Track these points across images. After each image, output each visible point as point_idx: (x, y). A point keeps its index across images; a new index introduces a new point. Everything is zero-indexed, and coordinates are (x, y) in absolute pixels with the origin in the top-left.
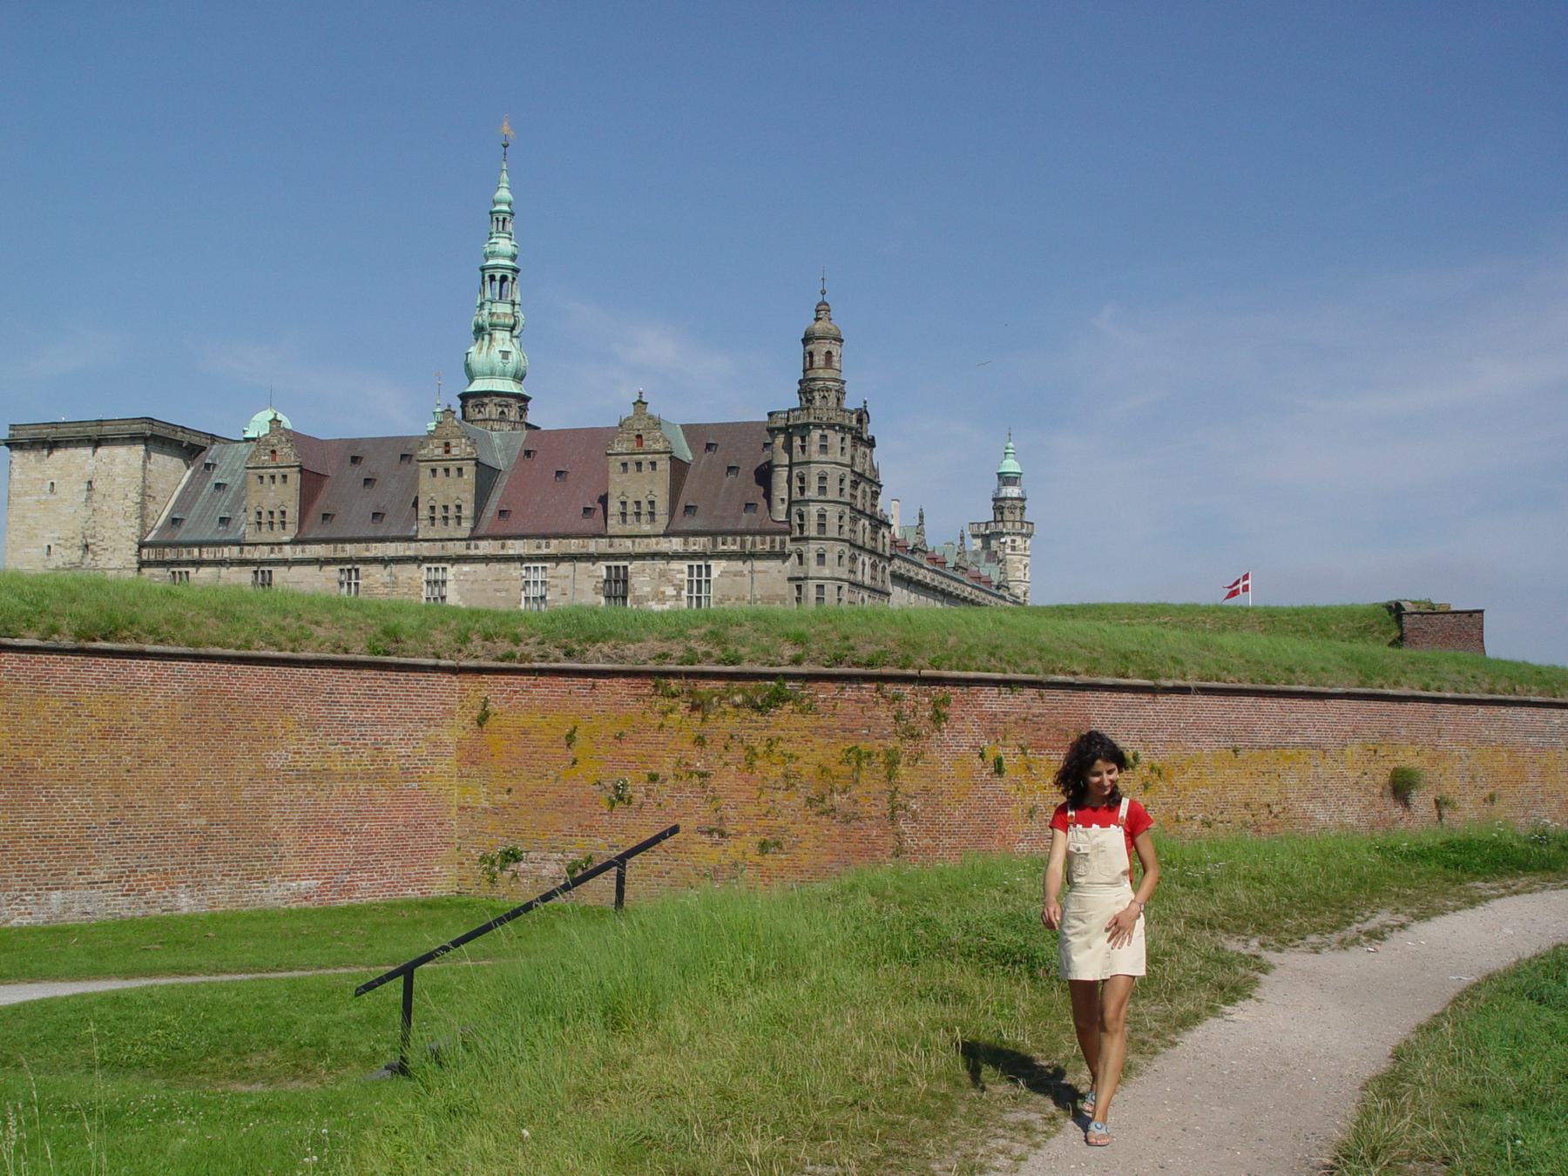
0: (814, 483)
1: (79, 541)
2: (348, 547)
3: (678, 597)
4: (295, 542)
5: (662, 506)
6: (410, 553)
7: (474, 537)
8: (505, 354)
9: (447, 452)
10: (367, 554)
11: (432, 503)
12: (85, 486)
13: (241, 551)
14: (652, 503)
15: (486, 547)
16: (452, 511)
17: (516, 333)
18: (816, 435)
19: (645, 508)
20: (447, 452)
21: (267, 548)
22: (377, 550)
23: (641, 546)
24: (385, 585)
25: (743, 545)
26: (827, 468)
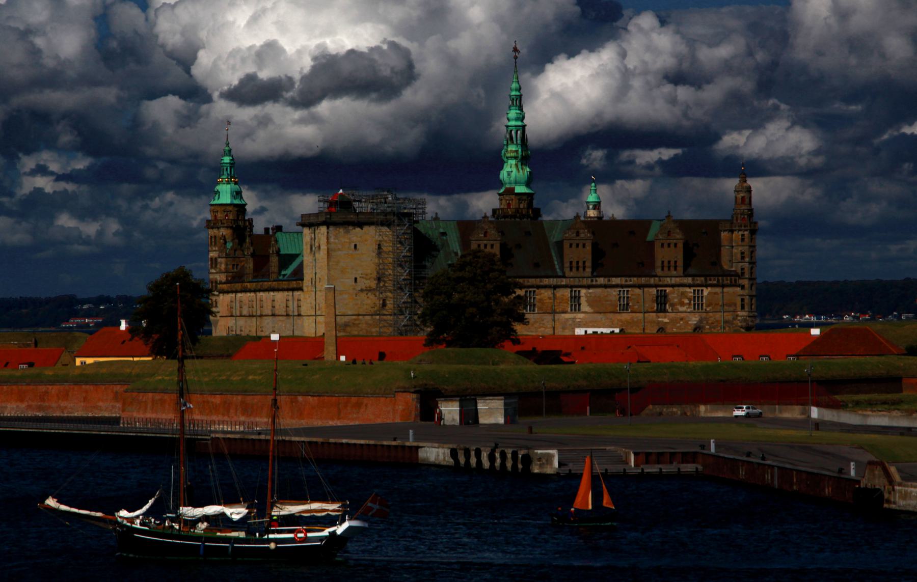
1: (375, 275)
2: (530, 280)
3: (690, 304)
6: (563, 283)
14: (676, 262)
16: (581, 264)
22: (546, 281)
23: (674, 281)
24: (550, 298)
25: (718, 280)
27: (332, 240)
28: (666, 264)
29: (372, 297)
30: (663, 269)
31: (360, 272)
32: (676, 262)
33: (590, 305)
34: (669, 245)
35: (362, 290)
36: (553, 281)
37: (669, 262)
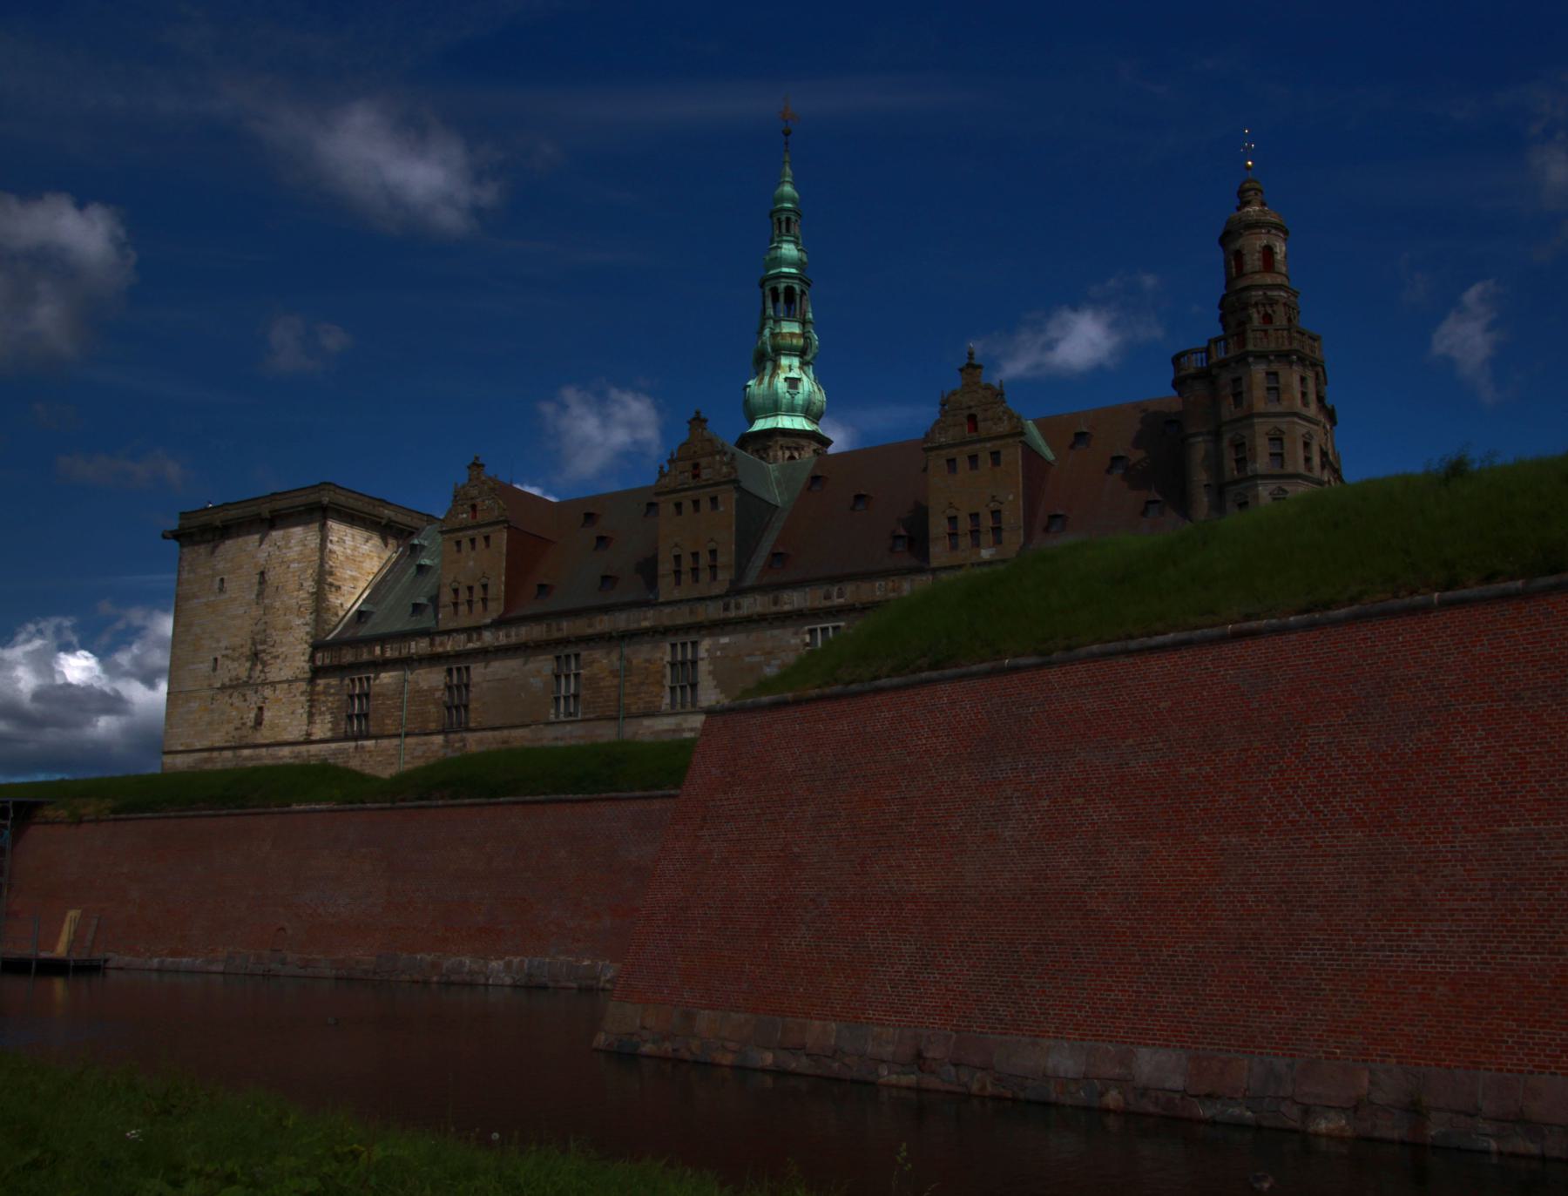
0: (1263, 447)
1: (246, 651)
4: (498, 624)
5: (1013, 516)
7: (737, 590)
8: (793, 383)
9: (696, 476)
10: (590, 631)
11: (676, 551)
12: (256, 579)
13: (432, 644)
14: (996, 514)
15: (752, 605)
16: (704, 560)
17: (808, 358)
18: (1258, 371)
19: (987, 522)
20: (696, 476)
21: (463, 637)
22: (603, 624)
24: (614, 673)
26: (1283, 423)
27: (185, 575)
28: (964, 525)
29: (237, 700)
30: (954, 547)
31: (223, 644)
32: (996, 514)
33: (722, 684)
34: (973, 459)
35: (223, 688)
36: (622, 621)
37: (974, 516)
